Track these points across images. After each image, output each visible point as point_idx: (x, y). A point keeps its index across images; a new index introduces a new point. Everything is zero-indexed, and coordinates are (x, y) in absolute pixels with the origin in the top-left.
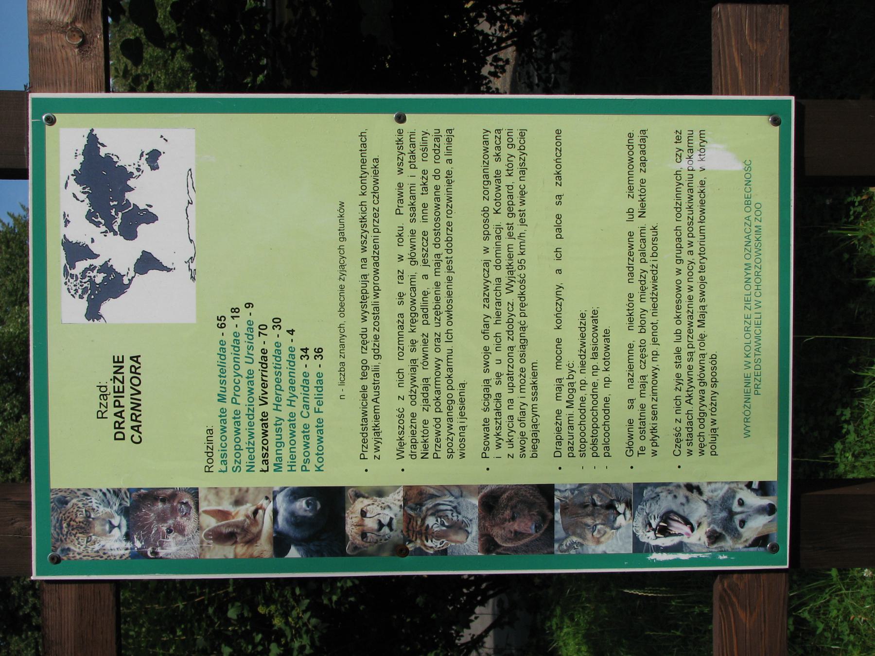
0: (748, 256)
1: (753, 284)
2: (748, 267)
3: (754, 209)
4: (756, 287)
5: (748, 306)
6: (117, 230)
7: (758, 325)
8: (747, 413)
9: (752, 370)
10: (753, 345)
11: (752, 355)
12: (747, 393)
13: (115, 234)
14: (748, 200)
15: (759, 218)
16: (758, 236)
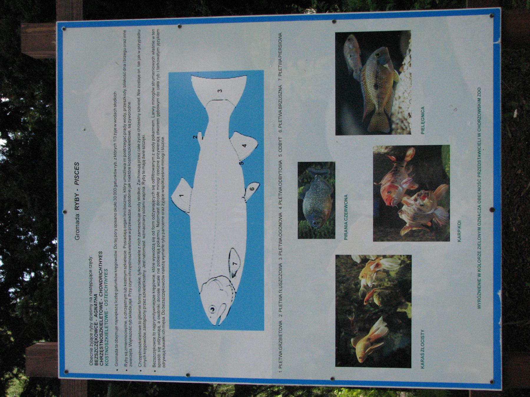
8: (479, 297)
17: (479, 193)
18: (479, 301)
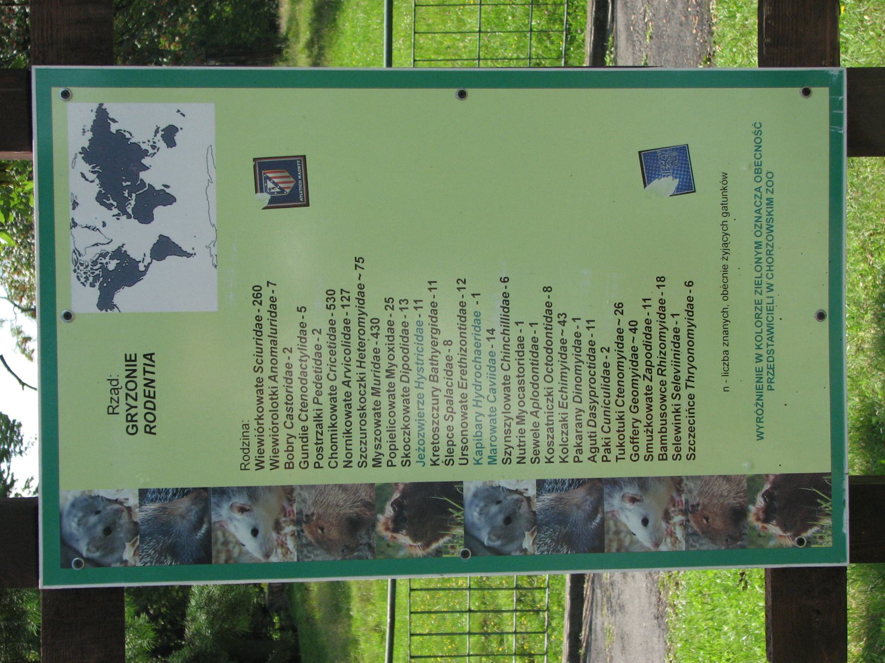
0: (758, 234)
1: (764, 265)
2: (758, 245)
3: (765, 179)
4: (768, 268)
5: (759, 290)
6: (130, 212)
7: (770, 311)
9: (764, 364)
10: (765, 335)
11: (764, 346)
12: (759, 389)
13: (129, 217)
14: (758, 167)
15: (771, 189)
16: (769, 210)
17: (758, 156)
18: (759, 420)
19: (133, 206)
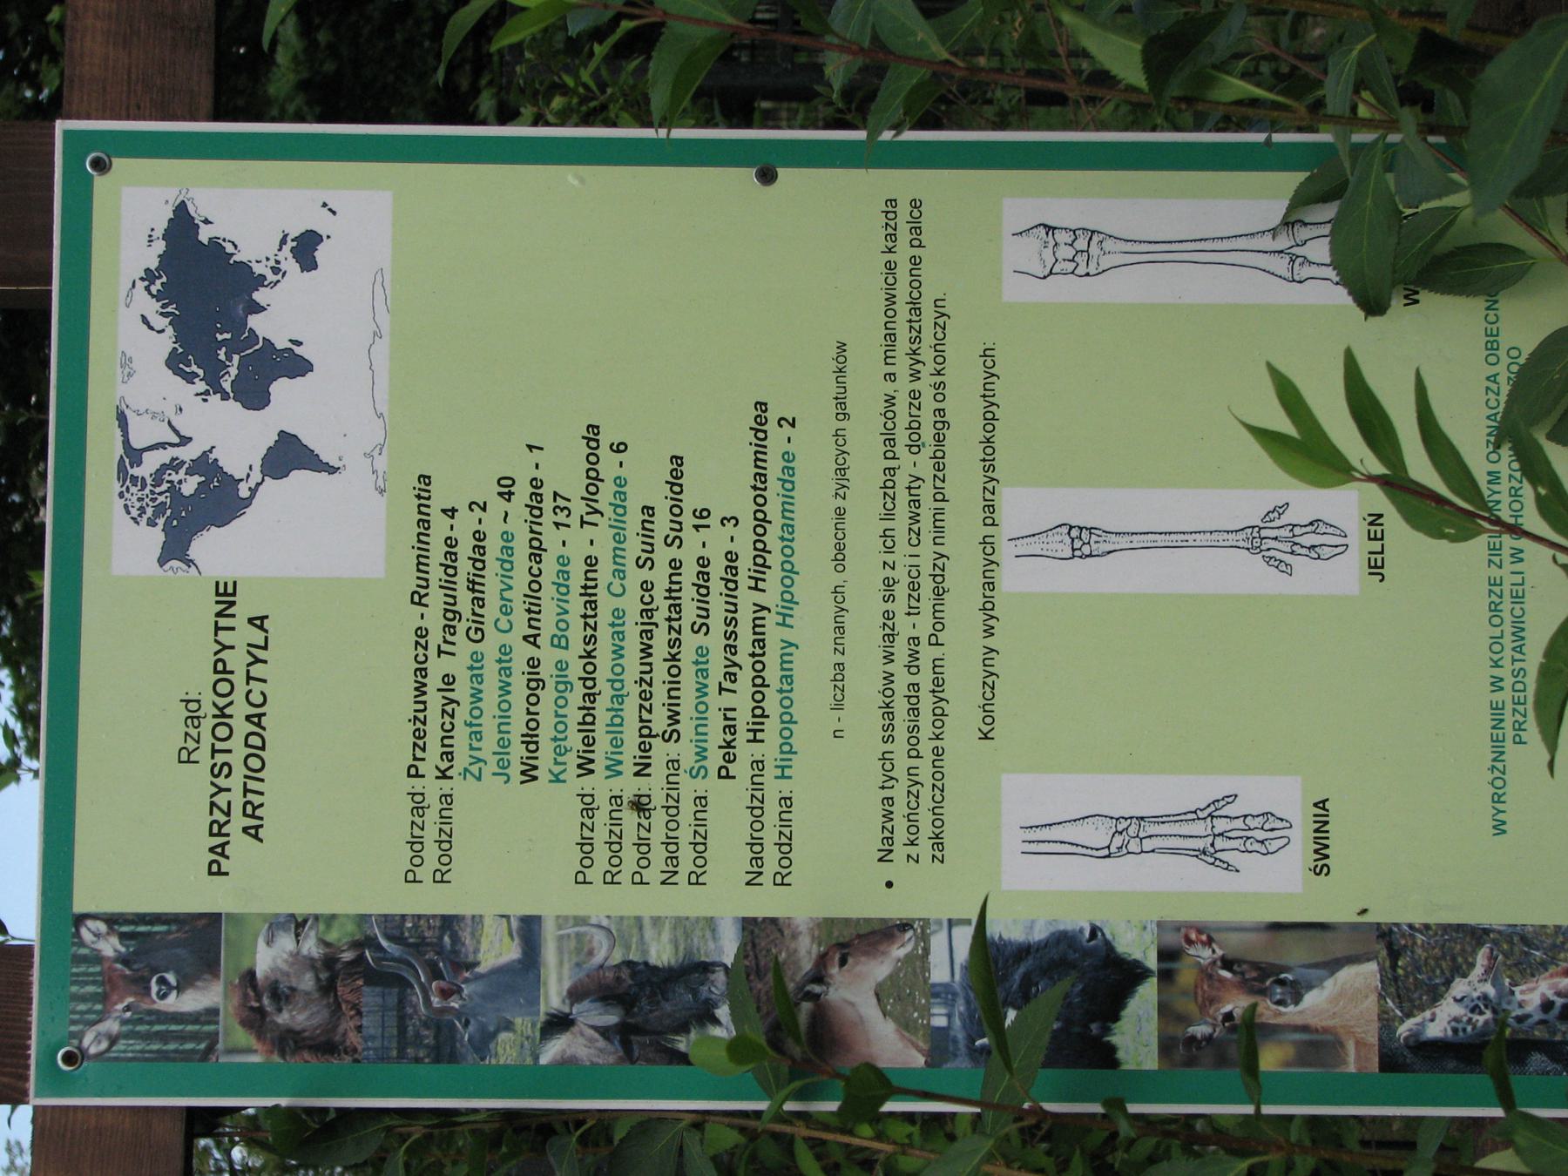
6: (228, 389)
13: (225, 397)
19: (233, 378)
